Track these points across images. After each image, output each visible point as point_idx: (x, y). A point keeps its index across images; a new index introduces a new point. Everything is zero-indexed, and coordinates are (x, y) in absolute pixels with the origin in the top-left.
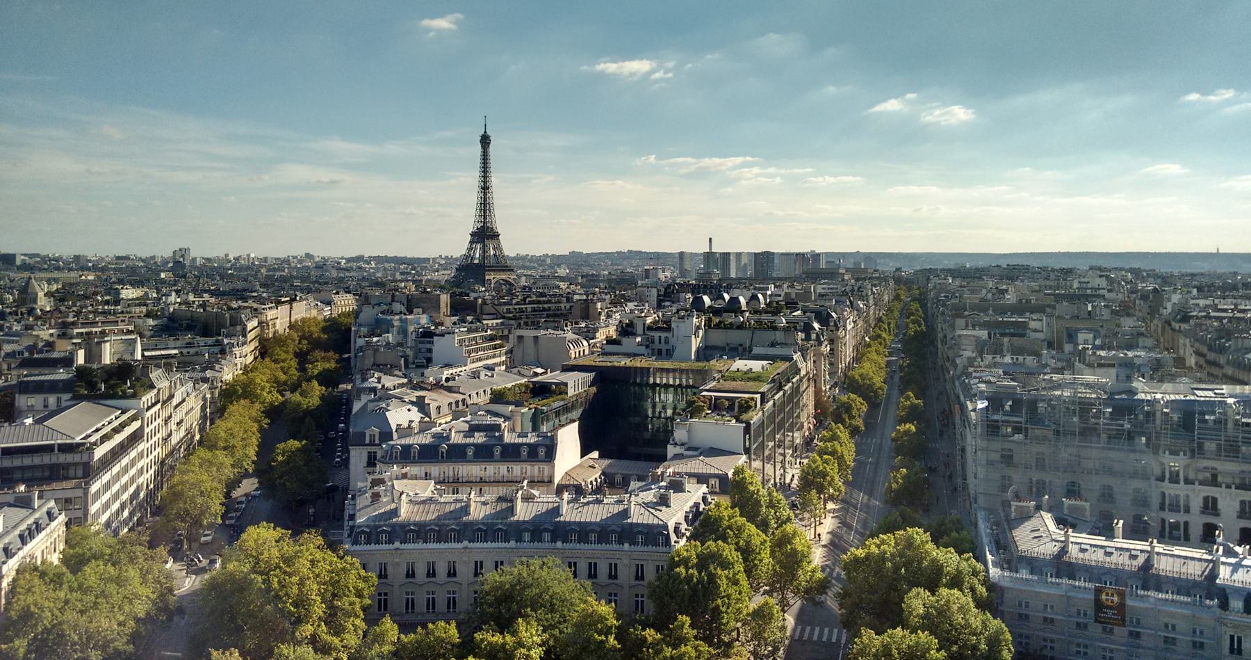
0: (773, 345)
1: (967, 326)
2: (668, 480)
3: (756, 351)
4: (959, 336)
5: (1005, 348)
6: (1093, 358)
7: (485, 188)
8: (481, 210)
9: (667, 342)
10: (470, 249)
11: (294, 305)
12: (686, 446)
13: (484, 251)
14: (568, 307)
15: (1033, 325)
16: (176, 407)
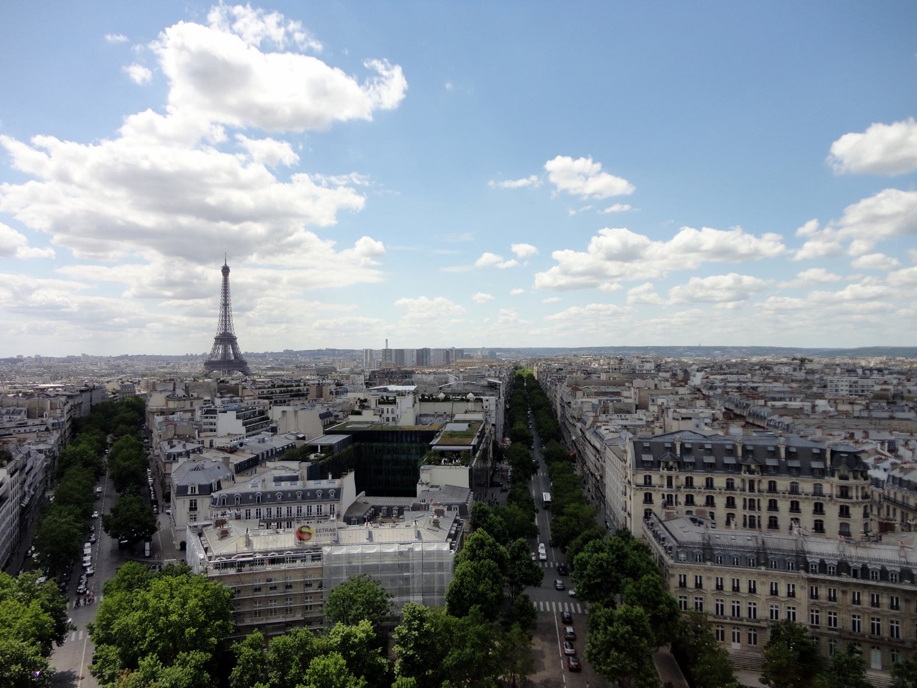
0: (466, 412)
1: (584, 395)
2: (434, 509)
3: (457, 417)
4: (582, 402)
5: (610, 410)
6: (675, 414)
7: (226, 305)
8: (222, 321)
9: (393, 412)
10: (214, 349)
11: (94, 392)
12: (430, 485)
13: (225, 350)
14: (305, 389)
15: (625, 393)
16: (27, 473)
